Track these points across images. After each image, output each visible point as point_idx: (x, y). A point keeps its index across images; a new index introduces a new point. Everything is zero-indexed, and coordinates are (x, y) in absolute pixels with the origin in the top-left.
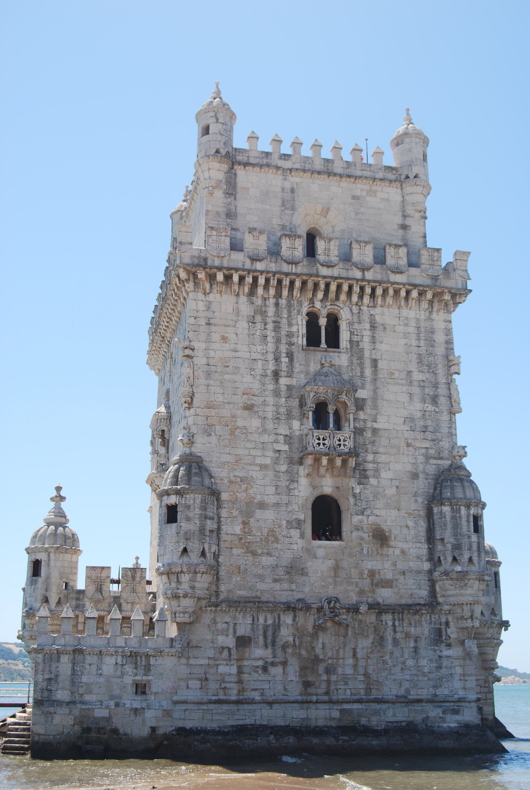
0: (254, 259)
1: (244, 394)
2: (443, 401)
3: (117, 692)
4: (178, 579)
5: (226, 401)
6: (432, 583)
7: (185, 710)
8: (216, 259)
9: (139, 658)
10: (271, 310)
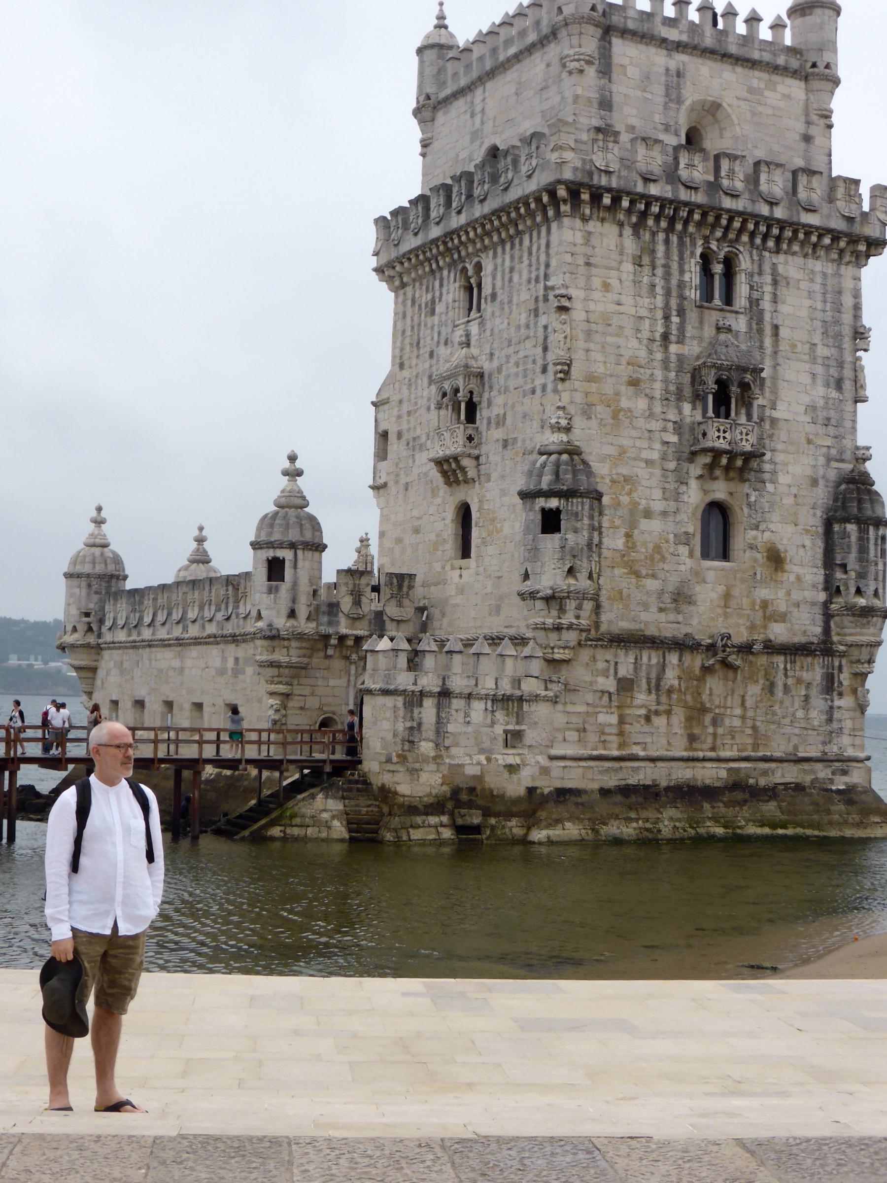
0: (647, 180)
1: (628, 364)
2: (848, 385)
3: (487, 745)
6: (828, 616)
7: (565, 767)
8: (603, 175)
10: (661, 248)
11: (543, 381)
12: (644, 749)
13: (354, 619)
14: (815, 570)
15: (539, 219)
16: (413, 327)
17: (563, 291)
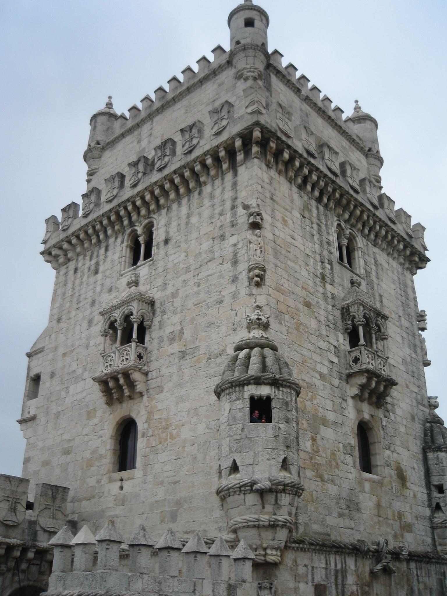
2: (419, 351)
4: (276, 500)
10: (315, 211)
11: (234, 289)
14: (422, 489)
15: (225, 166)
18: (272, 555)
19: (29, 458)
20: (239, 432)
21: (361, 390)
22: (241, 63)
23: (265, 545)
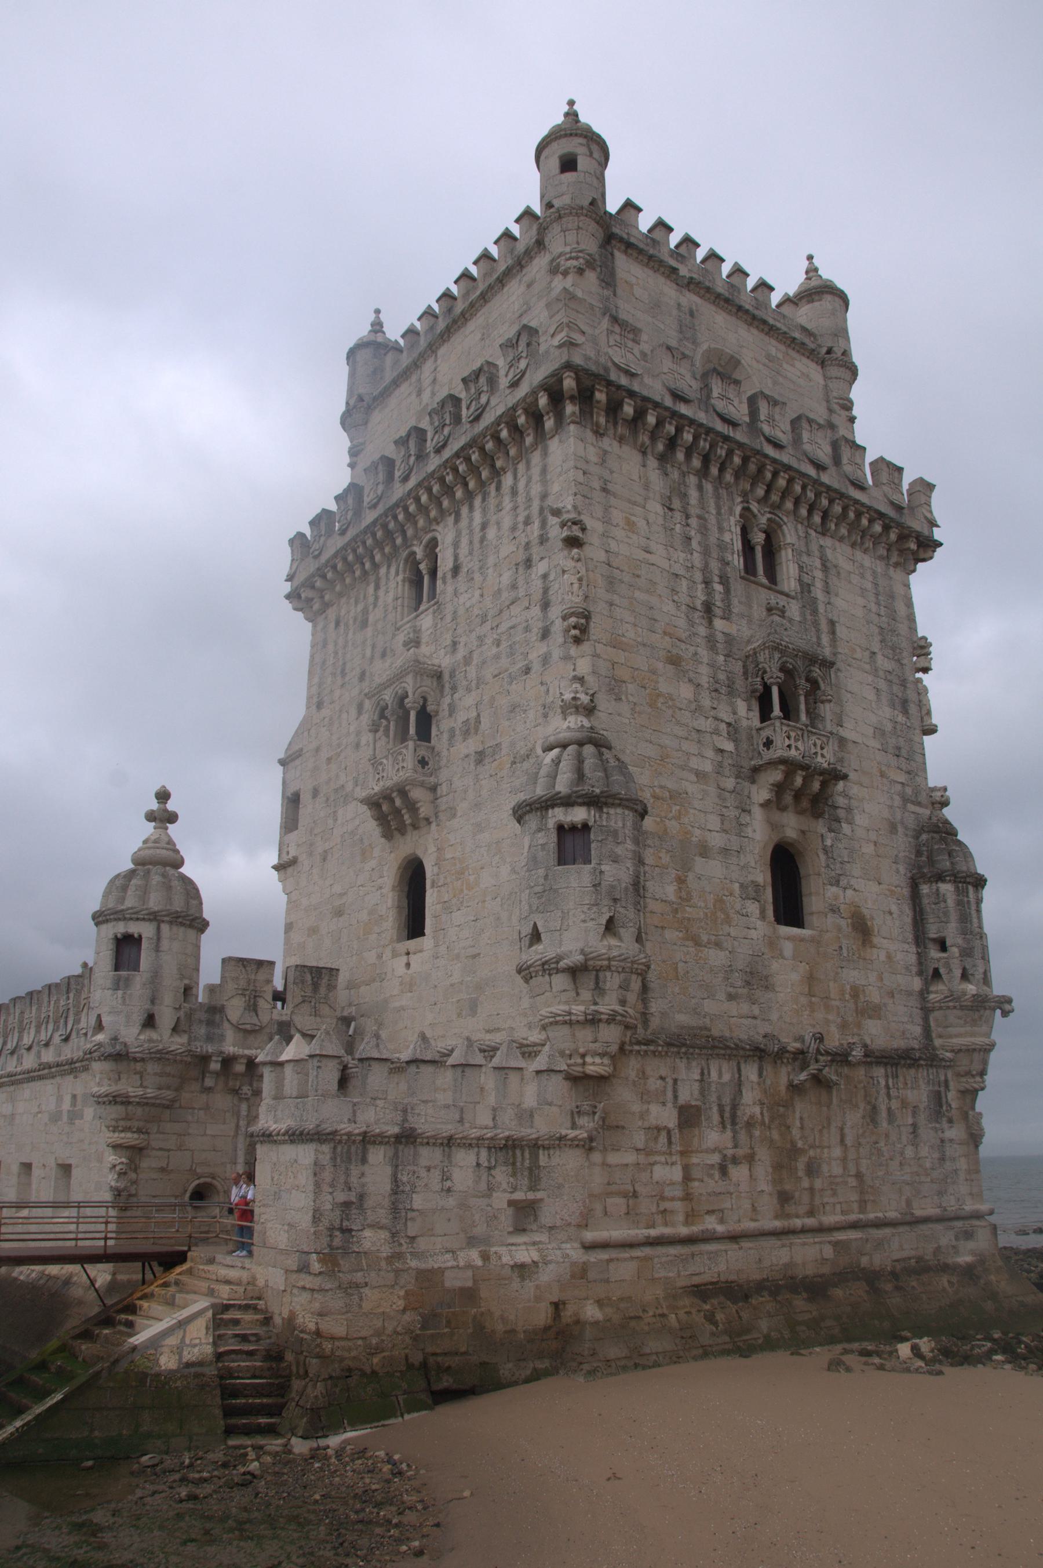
1: (665, 633)
2: (913, 709)
3: (480, 1230)
4: (597, 983)
5: (639, 639)
6: (926, 1011)
7: (611, 1260)
8: (622, 375)
9: (518, 1152)
10: (693, 494)
11: (545, 649)
12: (722, 1221)
13: (246, 1031)
14: (906, 946)
15: (529, 440)
16: (336, 653)
17: (573, 516)
18: (593, 1064)
19: (291, 923)
20: (541, 881)
21: (777, 792)
22: (557, 244)
23: (582, 1050)
